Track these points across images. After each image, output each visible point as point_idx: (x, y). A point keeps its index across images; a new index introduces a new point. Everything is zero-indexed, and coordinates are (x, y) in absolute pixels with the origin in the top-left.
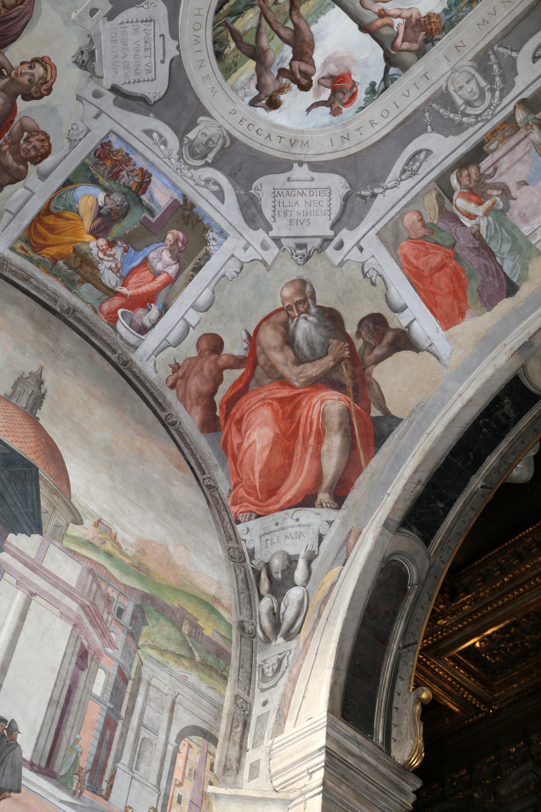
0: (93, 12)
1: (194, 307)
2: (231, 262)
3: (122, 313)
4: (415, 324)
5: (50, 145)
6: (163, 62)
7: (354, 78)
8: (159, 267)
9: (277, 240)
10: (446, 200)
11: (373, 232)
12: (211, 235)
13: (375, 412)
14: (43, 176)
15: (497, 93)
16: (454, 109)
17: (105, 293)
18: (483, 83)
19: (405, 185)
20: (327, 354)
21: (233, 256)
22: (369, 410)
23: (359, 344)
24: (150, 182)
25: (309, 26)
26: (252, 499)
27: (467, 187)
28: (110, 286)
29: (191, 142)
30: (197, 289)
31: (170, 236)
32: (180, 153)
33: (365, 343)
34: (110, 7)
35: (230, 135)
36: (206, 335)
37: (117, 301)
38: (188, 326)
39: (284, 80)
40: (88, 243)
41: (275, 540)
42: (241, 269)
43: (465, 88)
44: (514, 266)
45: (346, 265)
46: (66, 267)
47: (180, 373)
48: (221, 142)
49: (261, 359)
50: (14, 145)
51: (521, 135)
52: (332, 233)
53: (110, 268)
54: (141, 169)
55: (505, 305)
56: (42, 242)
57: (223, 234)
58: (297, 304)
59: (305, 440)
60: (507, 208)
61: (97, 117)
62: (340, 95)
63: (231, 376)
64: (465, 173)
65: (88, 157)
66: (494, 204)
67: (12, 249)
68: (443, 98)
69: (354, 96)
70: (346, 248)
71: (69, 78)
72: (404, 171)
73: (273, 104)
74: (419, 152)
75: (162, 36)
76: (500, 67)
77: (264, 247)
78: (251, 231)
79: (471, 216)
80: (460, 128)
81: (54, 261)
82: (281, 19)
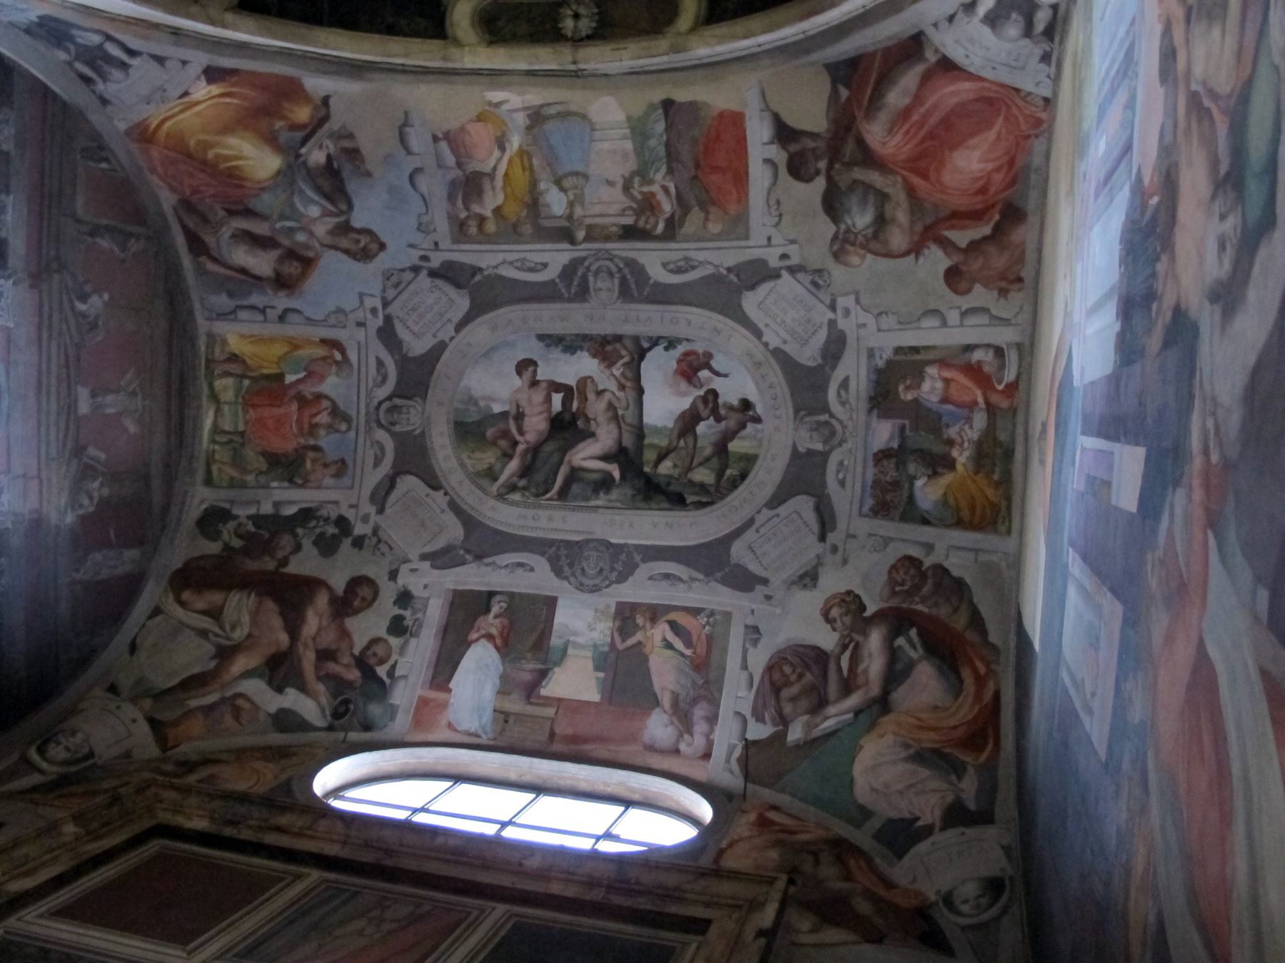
0: (768, 598)
1: (944, 324)
2: (884, 326)
3: (1000, 382)
4: (766, 139)
5: (899, 560)
6: (778, 515)
7: (675, 365)
8: (939, 385)
9: (833, 307)
10: (676, 218)
11: (751, 243)
12: (880, 363)
13: (844, 93)
14: (929, 547)
15: (586, 264)
16: (623, 281)
17: (995, 414)
18: (591, 279)
19: (701, 256)
20: (855, 181)
21: (879, 330)
22: (848, 99)
23: (822, 165)
24: (881, 451)
25: (672, 430)
26: (1015, 110)
27: (654, 214)
28: (985, 416)
29: (825, 443)
30: (929, 335)
31: (909, 397)
32: (840, 444)
33: (817, 158)
34: (758, 587)
35: (795, 419)
36: (956, 292)
37: (994, 399)
38: (964, 314)
39: (723, 412)
40: (964, 465)
41: (1003, 54)
42: (880, 314)
43: (605, 288)
44: (656, 122)
45: (791, 237)
46: (997, 469)
47: (1003, 284)
48: (807, 419)
49: (919, 227)
50: (909, 594)
51: (588, 221)
52: (784, 273)
53: (971, 427)
54: (876, 465)
55: (681, 96)
56: (988, 511)
57: (871, 353)
58: (853, 244)
59: (921, 123)
60: (634, 174)
61: (854, 536)
62: (695, 364)
63: (962, 237)
64: (648, 227)
65: (892, 519)
66: (642, 185)
67: (1009, 532)
68: (625, 294)
69: (687, 354)
70: (780, 251)
71: (833, 582)
72: (693, 268)
73: (746, 405)
74: (671, 271)
75: (757, 531)
76: (572, 280)
77: (847, 312)
78: (848, 332)
79: (666, 190)
80: (631, 263)
81: (998, 484)
82: (683, 452)
